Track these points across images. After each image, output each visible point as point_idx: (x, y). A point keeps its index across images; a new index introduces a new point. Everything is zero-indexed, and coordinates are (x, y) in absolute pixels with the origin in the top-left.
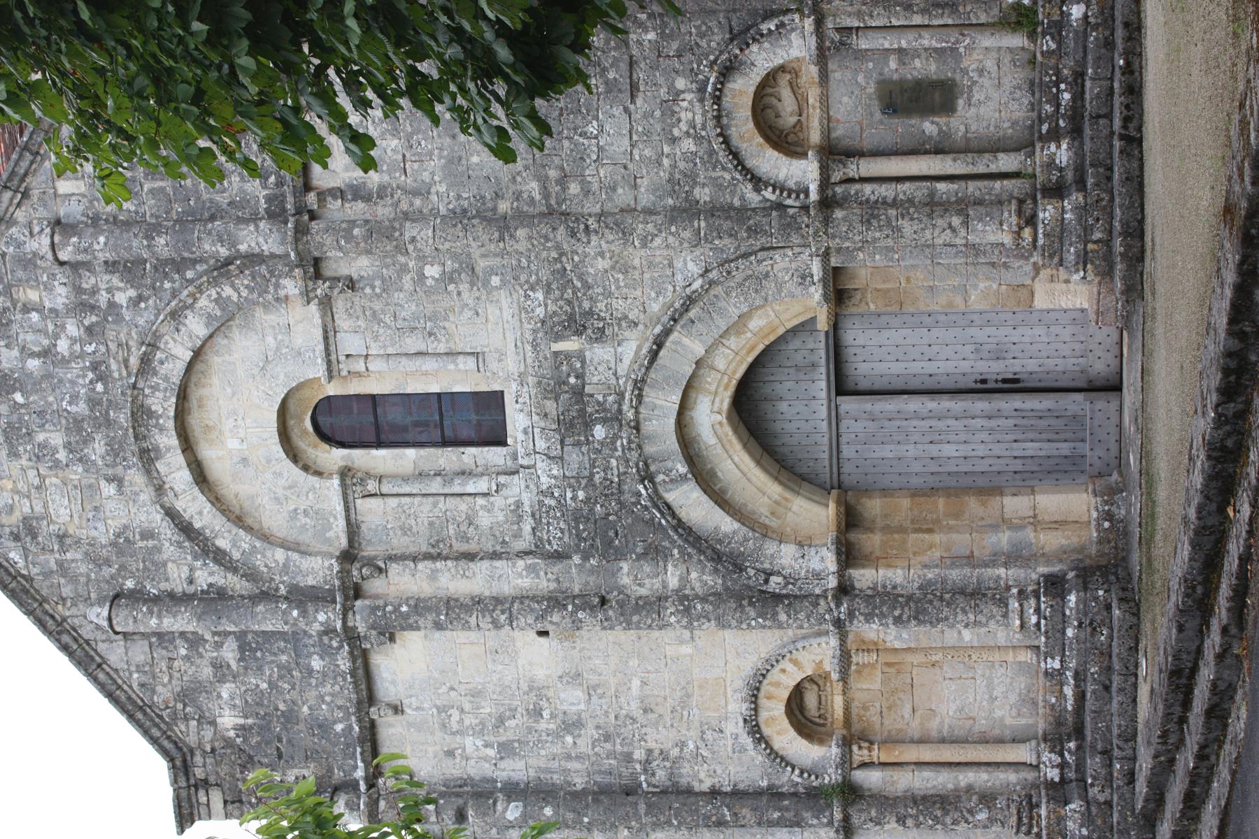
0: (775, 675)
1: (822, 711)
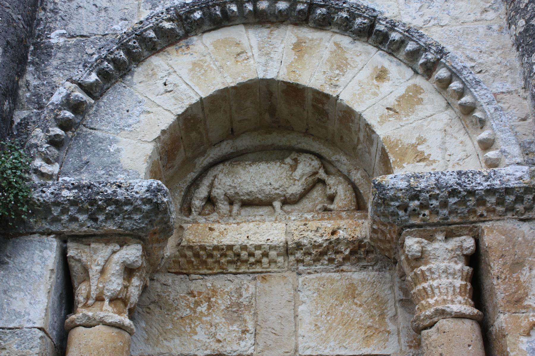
0: (366, 58)
1: (223, 207)
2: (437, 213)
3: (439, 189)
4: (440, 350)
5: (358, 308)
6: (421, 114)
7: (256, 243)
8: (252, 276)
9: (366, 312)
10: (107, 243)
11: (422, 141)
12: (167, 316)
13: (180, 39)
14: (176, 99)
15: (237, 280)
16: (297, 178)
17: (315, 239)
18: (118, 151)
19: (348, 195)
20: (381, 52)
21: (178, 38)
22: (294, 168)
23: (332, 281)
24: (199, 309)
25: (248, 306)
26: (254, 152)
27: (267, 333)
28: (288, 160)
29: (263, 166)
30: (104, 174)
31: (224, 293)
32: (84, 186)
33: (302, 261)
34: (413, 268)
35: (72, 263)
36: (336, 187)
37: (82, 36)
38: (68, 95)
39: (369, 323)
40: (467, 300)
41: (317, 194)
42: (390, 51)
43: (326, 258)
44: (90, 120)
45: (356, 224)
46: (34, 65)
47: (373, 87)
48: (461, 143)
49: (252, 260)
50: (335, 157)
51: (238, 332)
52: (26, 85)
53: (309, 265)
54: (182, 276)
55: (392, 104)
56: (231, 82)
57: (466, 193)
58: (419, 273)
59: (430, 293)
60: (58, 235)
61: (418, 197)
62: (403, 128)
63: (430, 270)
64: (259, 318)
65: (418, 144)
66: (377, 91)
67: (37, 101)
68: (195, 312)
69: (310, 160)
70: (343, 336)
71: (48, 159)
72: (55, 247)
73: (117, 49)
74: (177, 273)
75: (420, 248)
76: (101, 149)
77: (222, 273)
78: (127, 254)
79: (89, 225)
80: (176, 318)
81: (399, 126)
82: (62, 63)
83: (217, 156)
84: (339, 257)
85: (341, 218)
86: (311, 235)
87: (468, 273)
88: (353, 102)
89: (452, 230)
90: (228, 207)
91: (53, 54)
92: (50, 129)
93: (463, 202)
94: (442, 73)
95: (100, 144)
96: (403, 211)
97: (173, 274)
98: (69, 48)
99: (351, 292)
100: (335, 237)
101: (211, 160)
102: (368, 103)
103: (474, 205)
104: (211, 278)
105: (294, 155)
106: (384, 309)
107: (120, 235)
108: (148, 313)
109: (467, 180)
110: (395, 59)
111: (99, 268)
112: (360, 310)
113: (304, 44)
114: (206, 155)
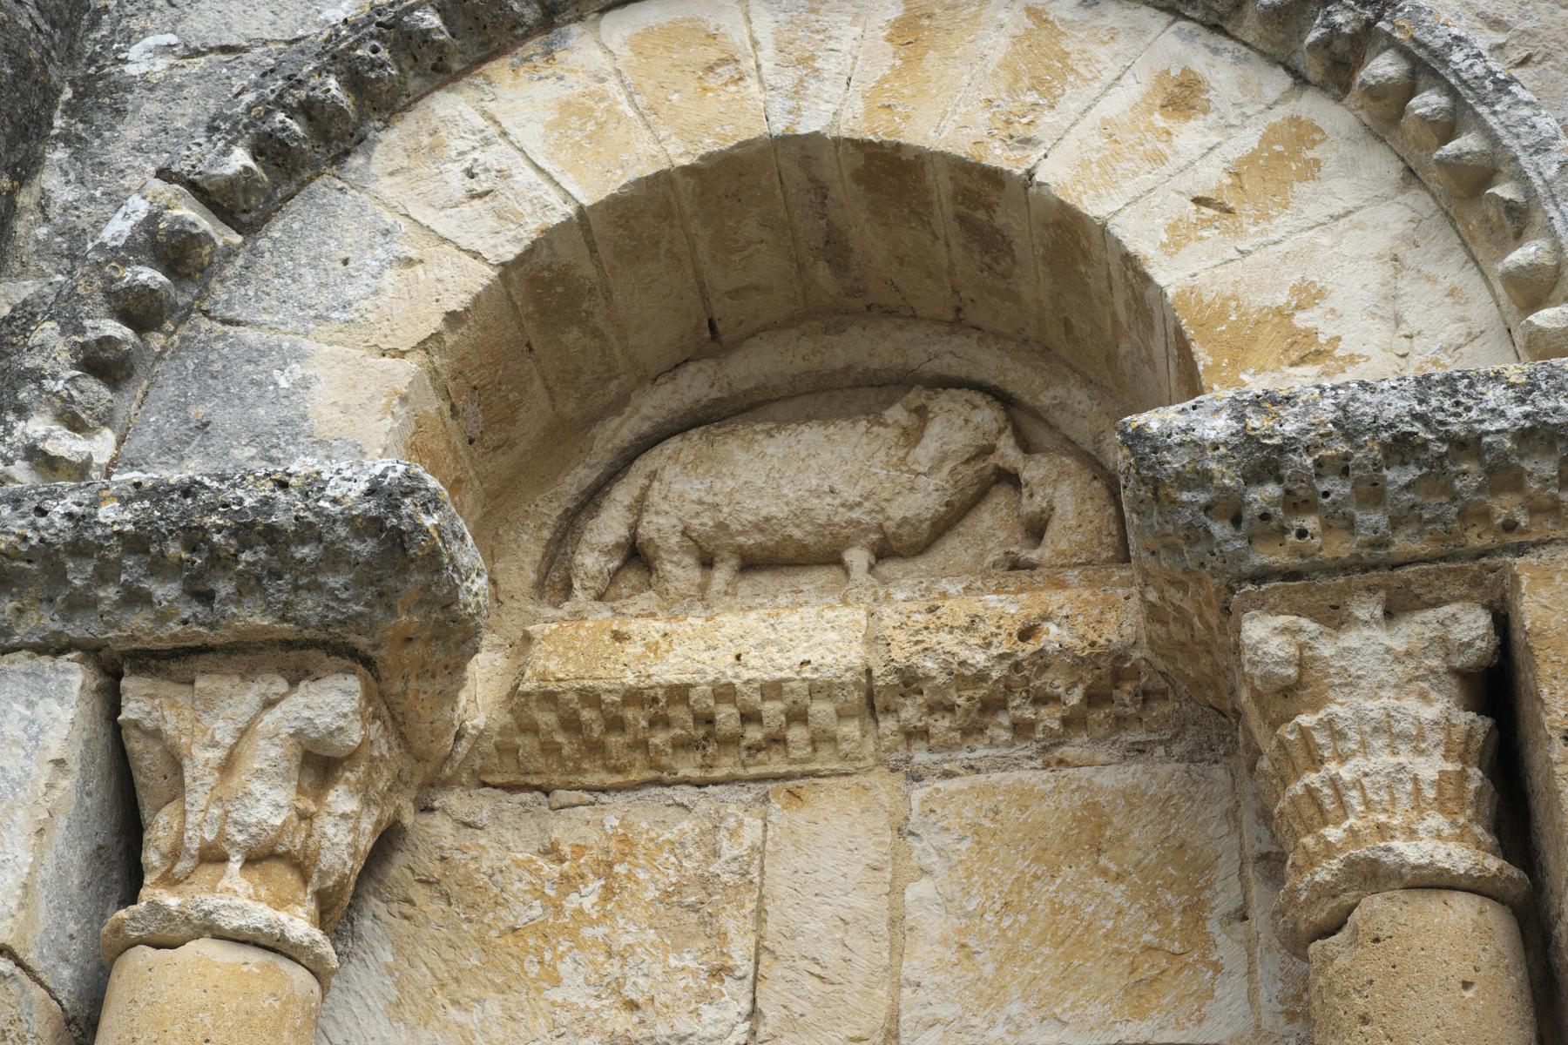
1: (680, 572)
2: (1350, 526)
3: (1349, 437)
4: (1360, 1001)
5: (1109, 888)
6: (1314, 212)
7: (766, 677)
8: (757, 789)
9: (1136, 900)
10: (249, 674)
11: (1309, 295)
12: (465, 926)
13: (527, 36)
14: (500, 217)
15: (704, 802)
16: (921, 469)
17: (964, 654)
18: (305, 384)
19: (1091, 513)
20: (1183, 24)
21: (520, 31)
22: (911, 437)
23: (1024, 797)
24: (572, 902)
25: (736, 887)
26: (790, 397)
27: (792, 975)
28: (897, 414)
29: (811, 434)
30: (252, 458)
31: (660, 848)
32: (173, 489)
33: (924, 734)
34: (1274, 725)
35: (135, 745)
36: (1049, 491)
37: (225, 49)
38: (153, 218)
39: (1147, 937)
40: (1463, 827)
41: (993, 523)
42: (1213, 19)
43: (1004, 719)
44: (225, 297)
45: (1104, 600)
46: (68, 145)
47: (1149, 136)
48: (1452, 293)
49: (754, 734)
50: (1052, 393)
51: (695, 974)
52: (39, 204)
53: (948, 747)
54: (526, 797)
55: (1214, 185)
56: (679, 153)
57: (1444, 449)
58: (1292, 737)
59: (1329, 805)
60: (92, 652)
61: (1277, 468)
62: (1249, 260)
63: (1328, 724)
64: (771, 928)
65: (1298, 307)
66: (1161, 146)
67: (69, 248)
68: (558, 910)
69: (968, 407)
70: (1054, 981)
71: (75, 417)
72: (76, 688)
73: (319, 71)
74: (511, 788)
75: (1293, 650)
76: (252, 382)
77: (659, 783)
78: (307, 707)
79: (186, 614)
80: (494, 933)
81: (1233, 254)
82: (155, 134)
83: (664, 413)
84: (1050, 718)
85: (1062, 585)
86: (948, 641)
87: (1470, 735)
88: (1080, 188)
89: (1408, 583)
90: (696, 575)
91: (130, 108)
92: (88, 323)
93: (1437, 476)
94: (1383, 67)
95: (250, 368)
96: (1227, 523)
97: (498, 791)
98: (181, 87)
99: (1091, 832)
100: (1031, 647)
101: (646, 427)
102: (1130, 188)
103: (1479, 490)
104: (620, 799)
105: (916, 397)
106: (1203, 888)
107: (288, 645)
108: (406, 917)
109: (1447, 404)
110: (1229, 44)
111: (215, 755)
112: (1117, 893)
113: (926, 22)
114: (628, 410)
